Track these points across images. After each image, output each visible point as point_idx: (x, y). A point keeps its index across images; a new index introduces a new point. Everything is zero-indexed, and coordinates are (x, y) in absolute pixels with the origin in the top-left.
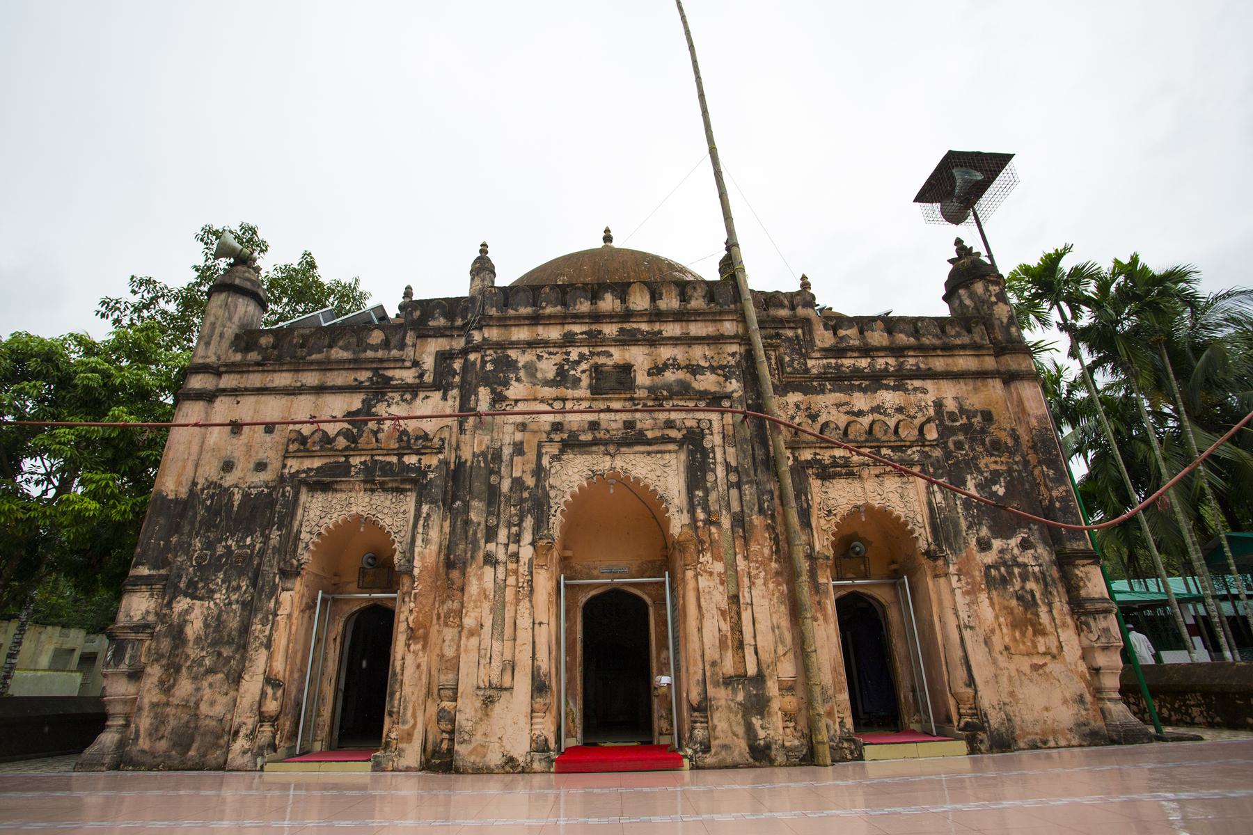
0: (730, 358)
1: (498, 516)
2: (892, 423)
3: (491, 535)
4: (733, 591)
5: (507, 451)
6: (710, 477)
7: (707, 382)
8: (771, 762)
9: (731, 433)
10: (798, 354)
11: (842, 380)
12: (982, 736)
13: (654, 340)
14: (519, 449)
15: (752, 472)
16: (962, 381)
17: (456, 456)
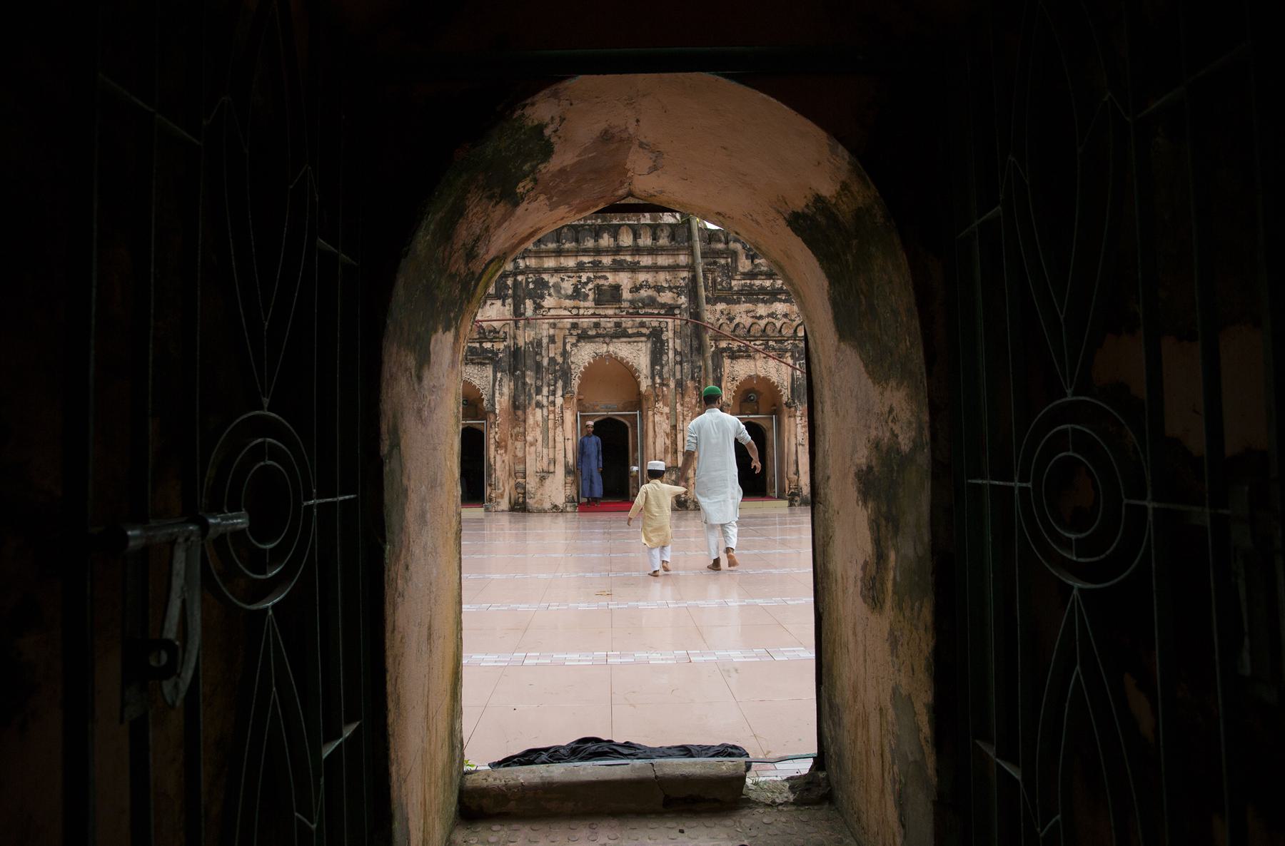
0: (682, 281)
1: (542, 380)
2: (778, 324)
3: (539, 391)
4: (673, 424)
5: (545, 341)
6: (665, 358)
7: (666, 297)
8: (687, 508)
9: (679, 331)
10: (726, 276)
11: (752, 295)
12: (797, 498)
13: (634, 268)
14: (552, 339)
15: (689, 355)
17: (514, 343)
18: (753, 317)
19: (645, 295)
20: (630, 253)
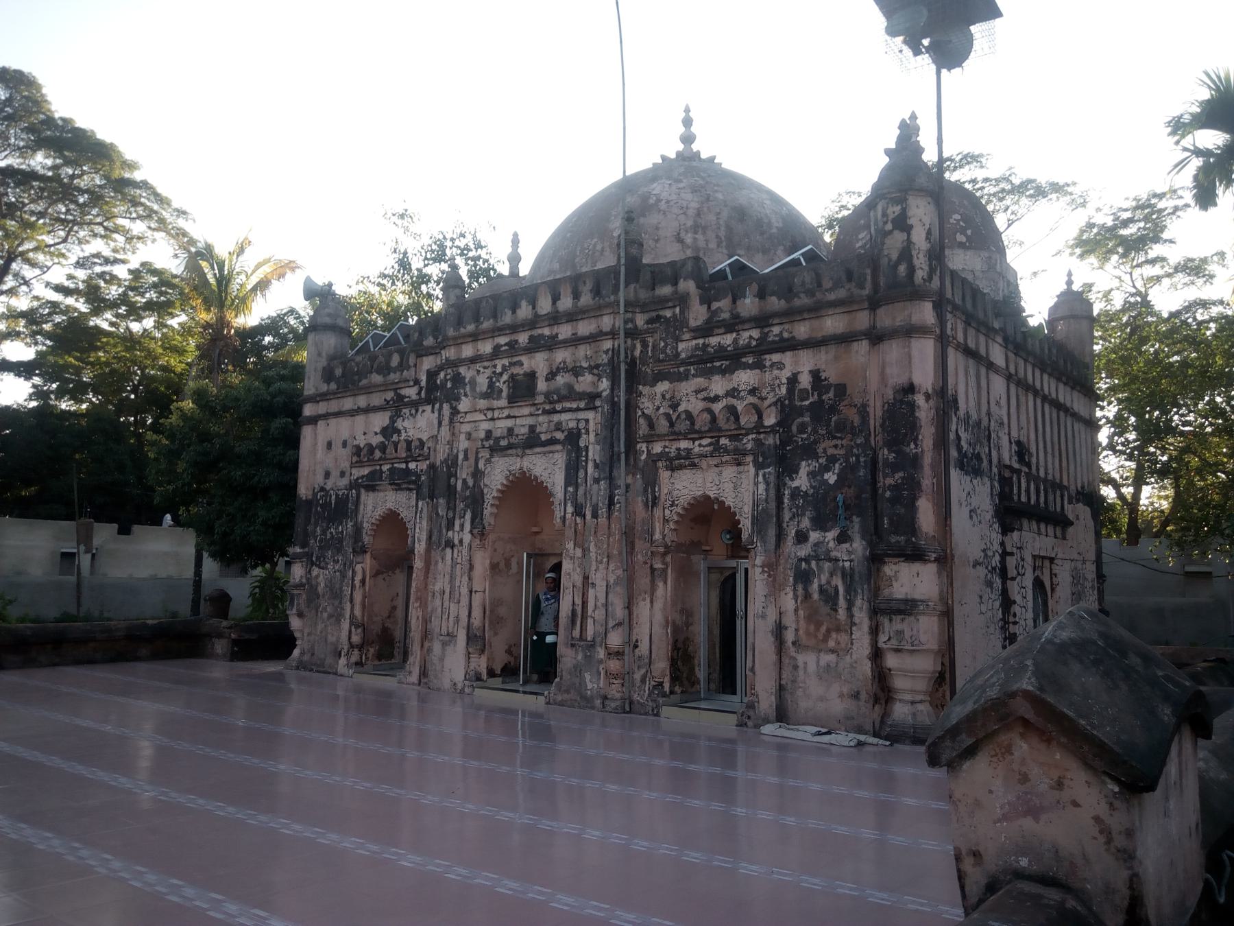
3: (450, 526)
6: (581, 474)
7: (585, 383)
11: (706, 362)
13: (551, 344)
16: (823, 348)
18: (704, 399)
19: (562, 382)
20: (547, 323)
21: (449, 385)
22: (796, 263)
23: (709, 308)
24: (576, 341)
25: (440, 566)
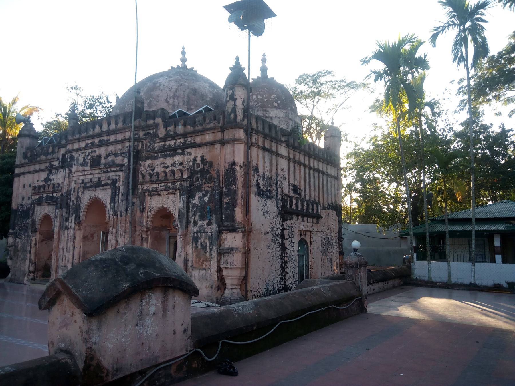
3: (67, 220)
6: (117, 198)
7: (119, 160)
13: (106, 143)
16: (205, 147)
18: (163, 167)
21: (69, 160)
22: (200, 112)
23: (166, 129)
24: (116, 142)
25: (63, 237)
